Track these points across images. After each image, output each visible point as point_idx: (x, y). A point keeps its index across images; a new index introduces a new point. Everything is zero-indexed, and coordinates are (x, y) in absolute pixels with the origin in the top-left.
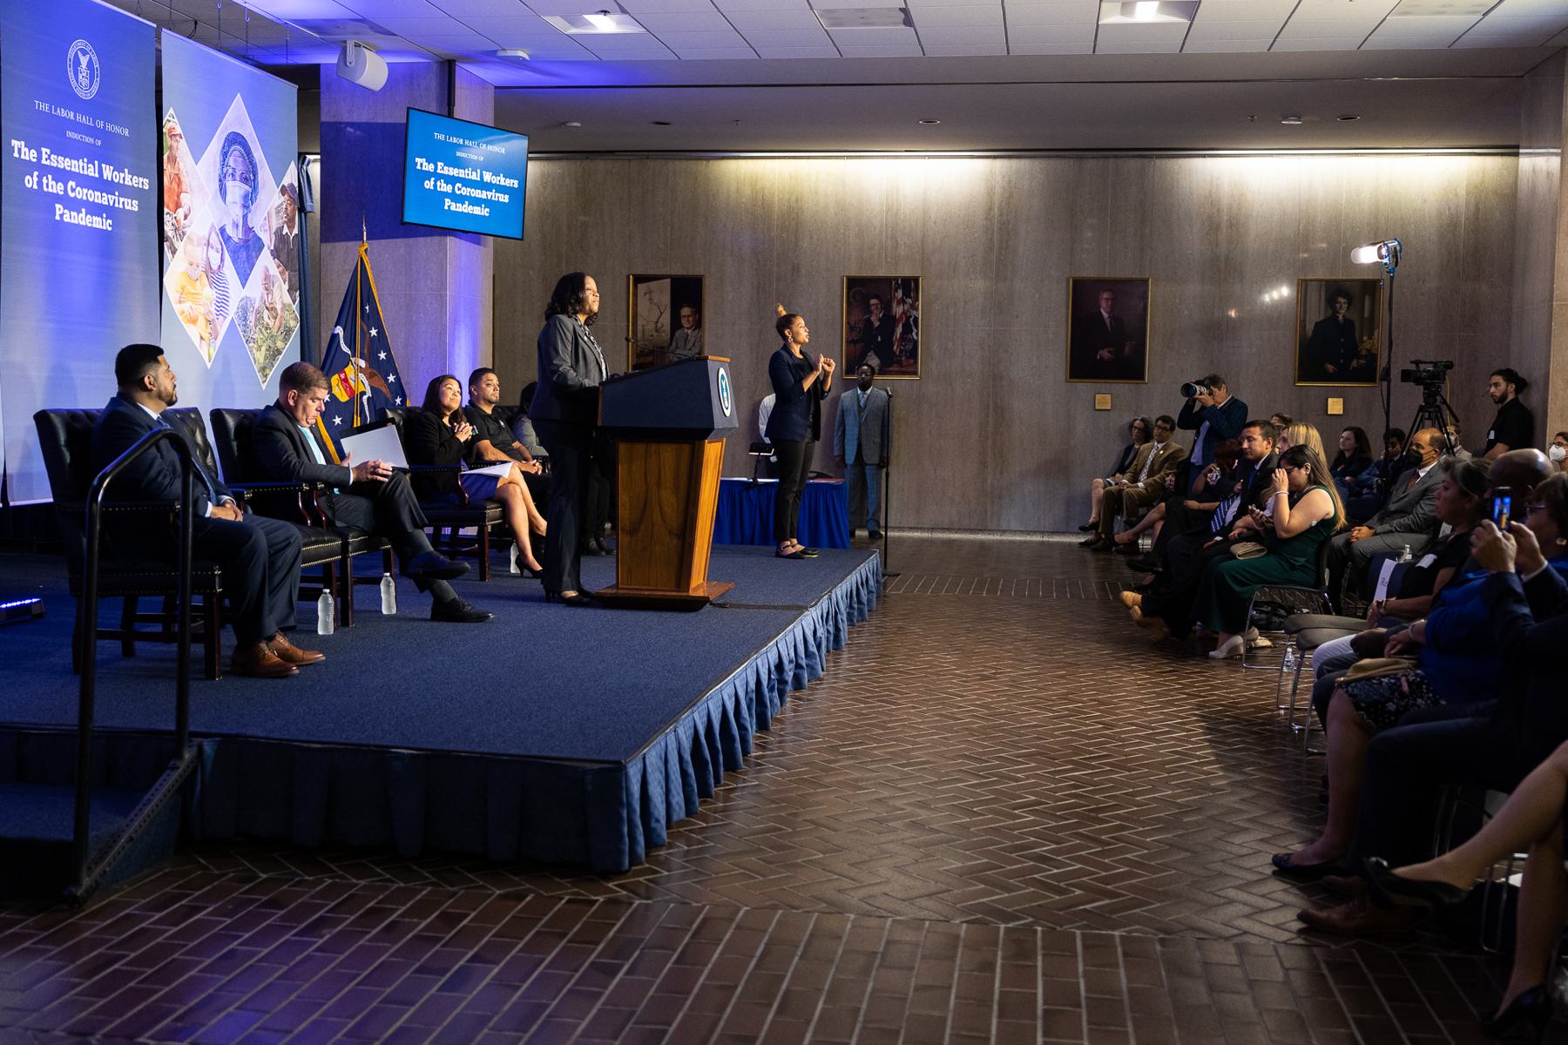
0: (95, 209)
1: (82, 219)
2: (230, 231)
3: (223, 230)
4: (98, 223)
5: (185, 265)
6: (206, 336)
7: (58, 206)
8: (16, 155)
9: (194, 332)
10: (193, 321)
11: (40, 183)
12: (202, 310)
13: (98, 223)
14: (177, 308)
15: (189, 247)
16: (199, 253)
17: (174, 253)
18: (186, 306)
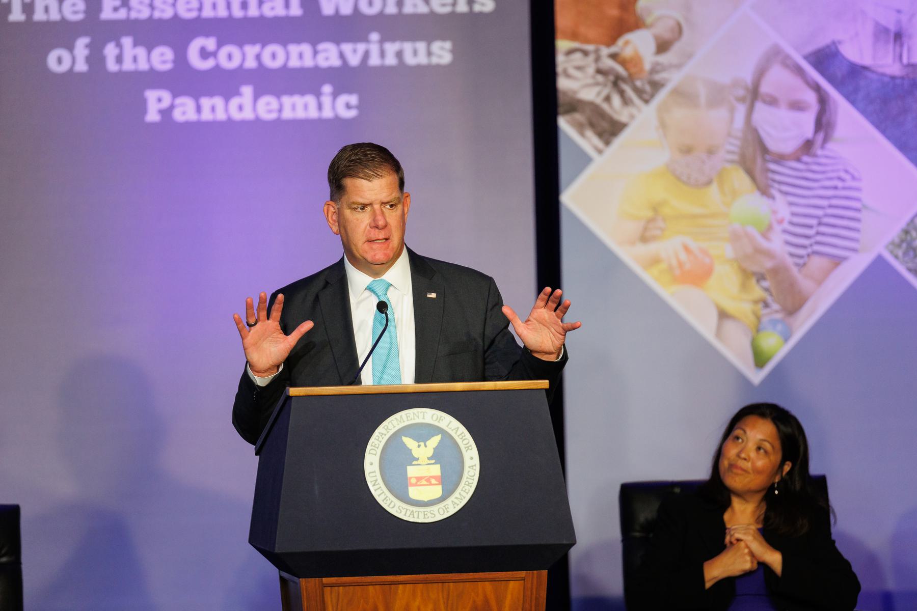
0: (305, 81)
1: (245, 106)
2: (858, 50)
3: (824, 59)
4: (299, 107)
5: (662, 157)
6: (742, 306)
7: (151, 96)
8: (17, 15)
9: (695, 308)
10: (697, 275)
11: (96, 58)
12: (727, 250)
13: (299, 107)
14: (630, 256)
15: (680, 115)
16: (723, 124)
17: (609, 130)
18: (669, 247)
